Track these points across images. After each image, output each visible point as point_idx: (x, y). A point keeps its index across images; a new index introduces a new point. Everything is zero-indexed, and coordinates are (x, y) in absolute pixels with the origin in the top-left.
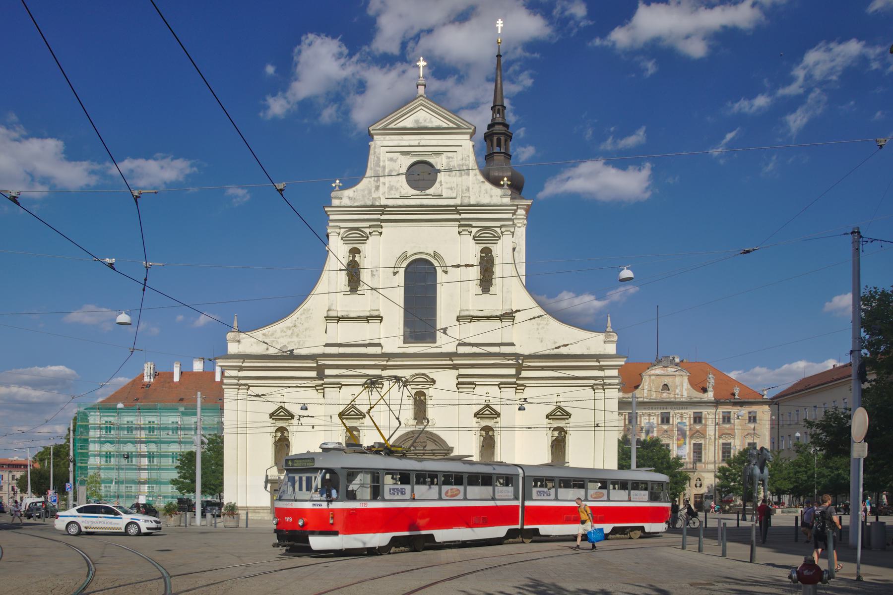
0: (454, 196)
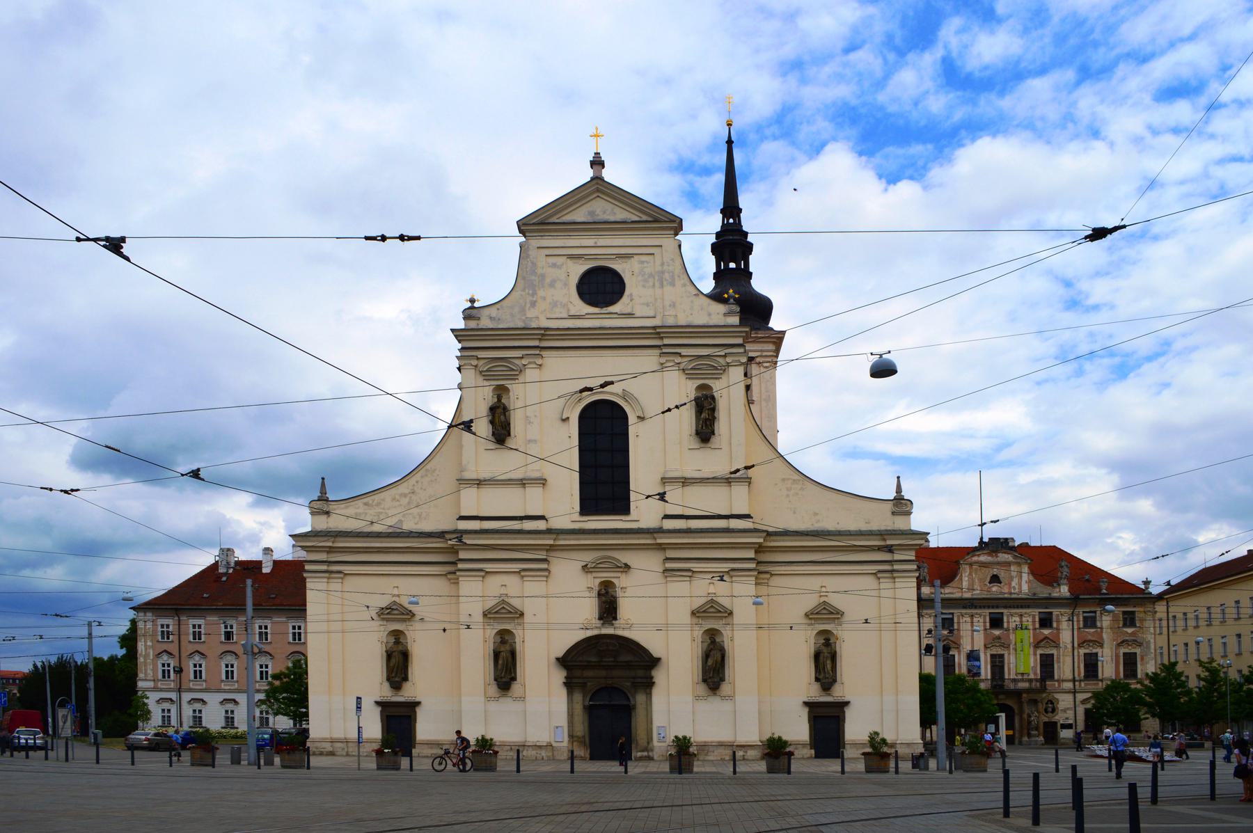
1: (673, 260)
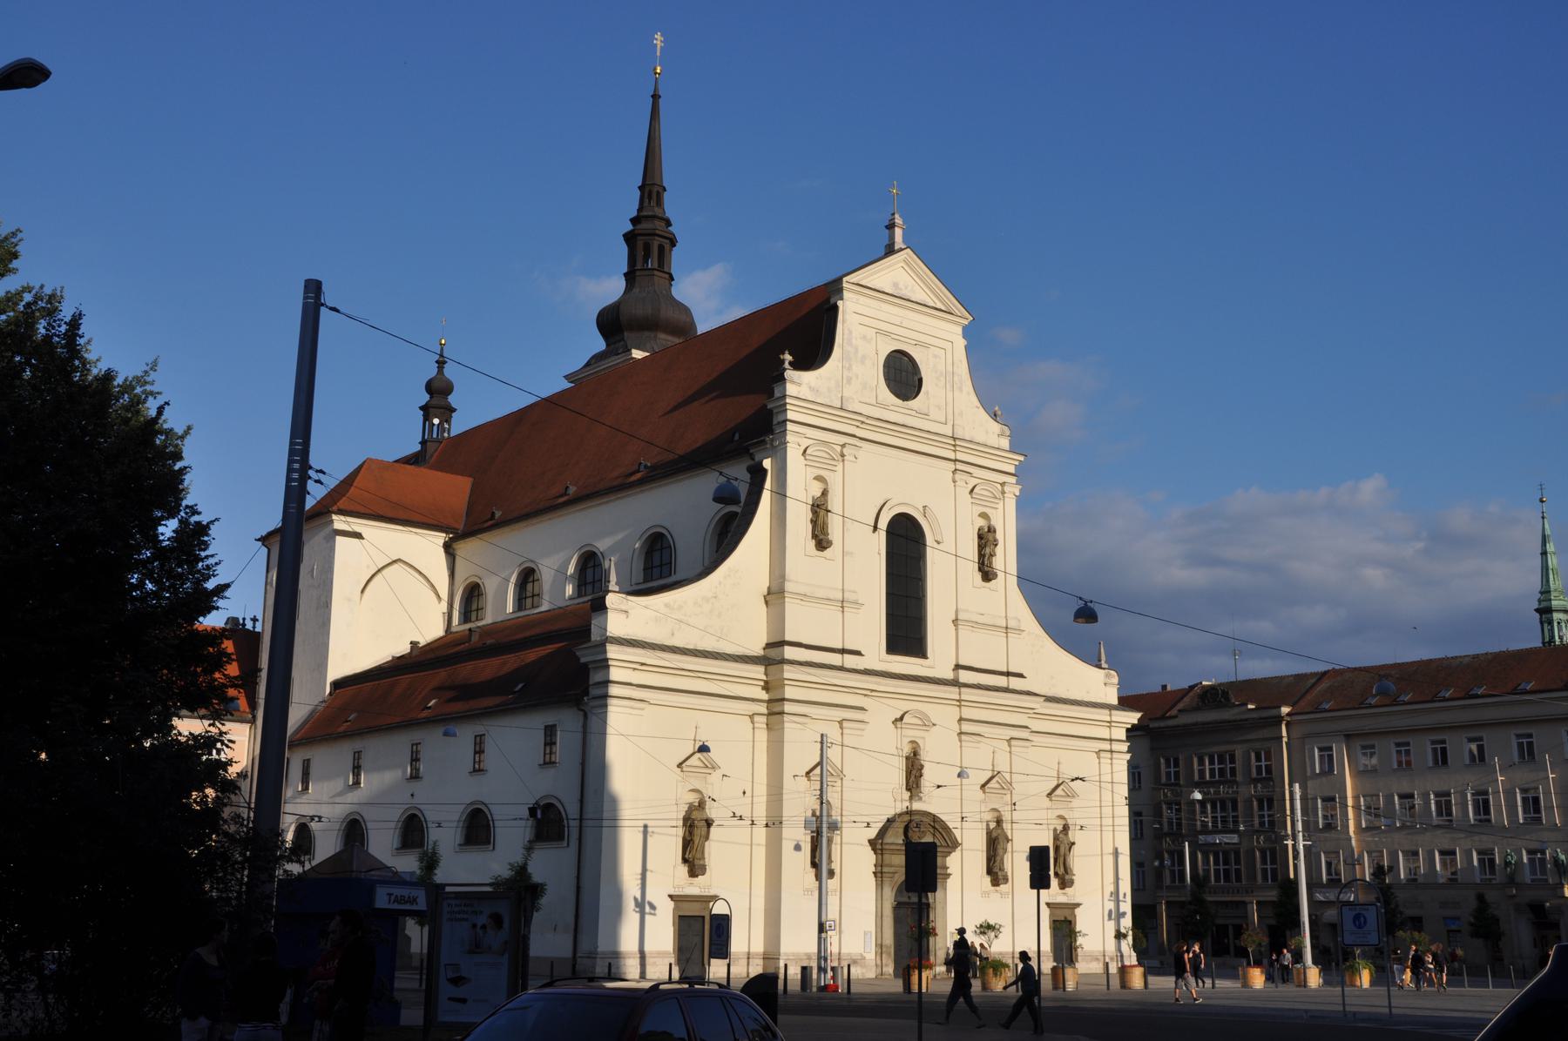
0: (943, 420)
1: (961, 361)
